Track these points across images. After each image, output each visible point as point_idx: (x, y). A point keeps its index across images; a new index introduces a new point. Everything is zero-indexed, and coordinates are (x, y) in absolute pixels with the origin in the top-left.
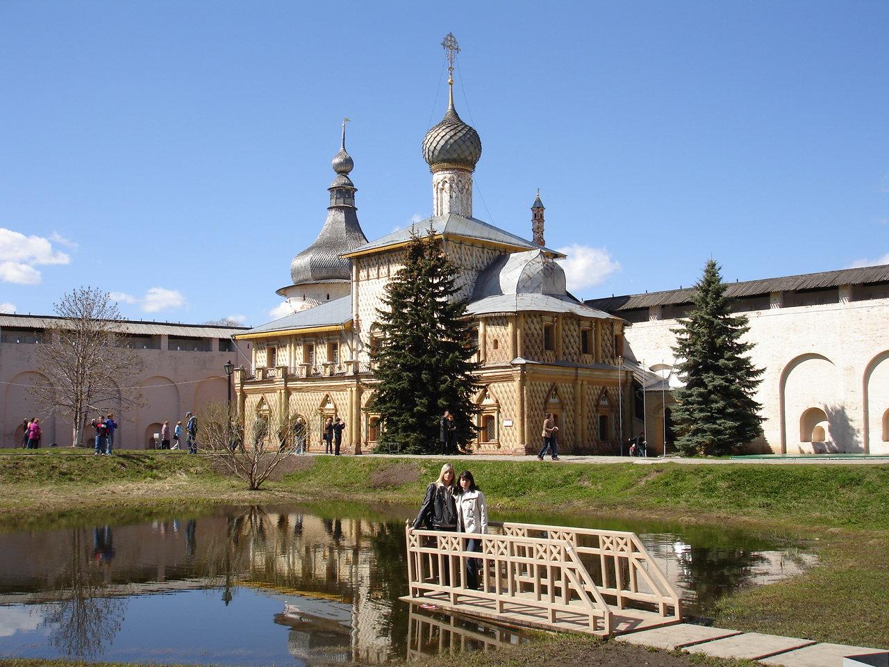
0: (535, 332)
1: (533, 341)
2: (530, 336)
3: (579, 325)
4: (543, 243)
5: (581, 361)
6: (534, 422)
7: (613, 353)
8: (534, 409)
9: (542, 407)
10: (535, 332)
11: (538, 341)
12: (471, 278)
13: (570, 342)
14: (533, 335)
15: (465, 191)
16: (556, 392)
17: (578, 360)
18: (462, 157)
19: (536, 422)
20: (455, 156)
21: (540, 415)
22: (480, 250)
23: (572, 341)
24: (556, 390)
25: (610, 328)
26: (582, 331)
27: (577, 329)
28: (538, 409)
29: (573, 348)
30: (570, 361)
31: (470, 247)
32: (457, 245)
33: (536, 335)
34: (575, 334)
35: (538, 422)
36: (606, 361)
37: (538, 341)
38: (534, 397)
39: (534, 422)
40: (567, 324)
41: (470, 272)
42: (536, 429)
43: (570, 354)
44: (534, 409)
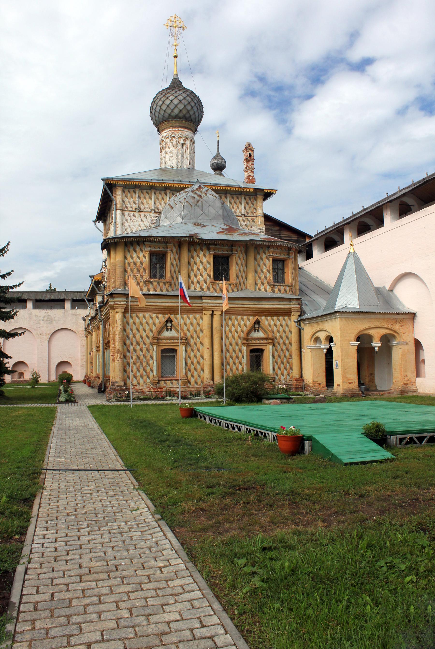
0: (138, 260)
1: (135, 271)
2: (132, 264)
3: (209, 249)
4: (253, 181)
5: (212, 289)
6: (135, 357)
7: (270, 279)
8: (135, 344)
9: (148, 341)
10: (138, 260)
11: (142, 270)
12: (149, 219)
13: (198, 269)
14: (135, 263)
15: (180, 146)
16: (172, 324)
17: (209, 289)
18: (173, 114)
19: (138, 357)
20: (166, 115)
21: (145, 350)
22: (163, 193)
23: (201, 267)
24: (171, 321)
25: (267, 252)
26: (215, 257)
27: (207, 254)
28: (141, 344)
29: (202, 275)
30: (199, 289)
31: (149, 191)
32: (132, 191)
33: (138, 264)
34: (205, 260)
35: (142, 357)
36: (262, 288)
37: (142, 270)
38: (135, 331)
39: (135, 357)
40: (195, 250)
41: (147, 214)
42: (138, 364)
43: (199, 282)
44: (135, 344)
